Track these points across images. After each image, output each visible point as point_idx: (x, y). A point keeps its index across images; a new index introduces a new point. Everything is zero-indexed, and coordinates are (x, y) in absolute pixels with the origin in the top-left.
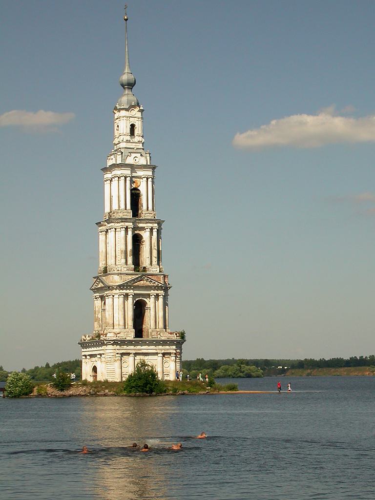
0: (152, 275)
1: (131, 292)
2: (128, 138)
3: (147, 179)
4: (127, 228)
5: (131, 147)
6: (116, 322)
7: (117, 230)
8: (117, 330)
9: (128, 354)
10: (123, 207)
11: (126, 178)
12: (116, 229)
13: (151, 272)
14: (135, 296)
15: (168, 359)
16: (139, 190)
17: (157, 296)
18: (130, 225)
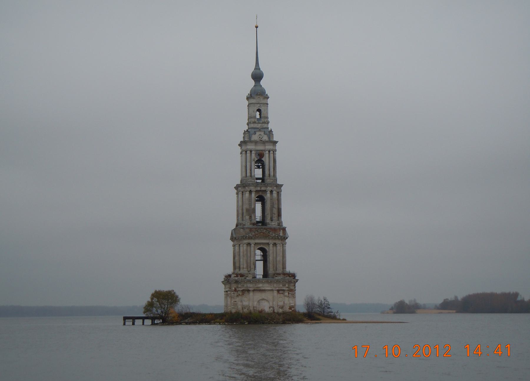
0: (271, 229)
1: (252, 242)
3: (269, 151)
4: (250, 192)
6: (241, 266)
8: (242, 271)
9: (248, 291)
10: (248, 174)
11: (251, 151)
12: (243, 192)
14: (256, 244)
15: (282, 295)
16: (262, 161)
17: (275, 244)
18: (253, 188)
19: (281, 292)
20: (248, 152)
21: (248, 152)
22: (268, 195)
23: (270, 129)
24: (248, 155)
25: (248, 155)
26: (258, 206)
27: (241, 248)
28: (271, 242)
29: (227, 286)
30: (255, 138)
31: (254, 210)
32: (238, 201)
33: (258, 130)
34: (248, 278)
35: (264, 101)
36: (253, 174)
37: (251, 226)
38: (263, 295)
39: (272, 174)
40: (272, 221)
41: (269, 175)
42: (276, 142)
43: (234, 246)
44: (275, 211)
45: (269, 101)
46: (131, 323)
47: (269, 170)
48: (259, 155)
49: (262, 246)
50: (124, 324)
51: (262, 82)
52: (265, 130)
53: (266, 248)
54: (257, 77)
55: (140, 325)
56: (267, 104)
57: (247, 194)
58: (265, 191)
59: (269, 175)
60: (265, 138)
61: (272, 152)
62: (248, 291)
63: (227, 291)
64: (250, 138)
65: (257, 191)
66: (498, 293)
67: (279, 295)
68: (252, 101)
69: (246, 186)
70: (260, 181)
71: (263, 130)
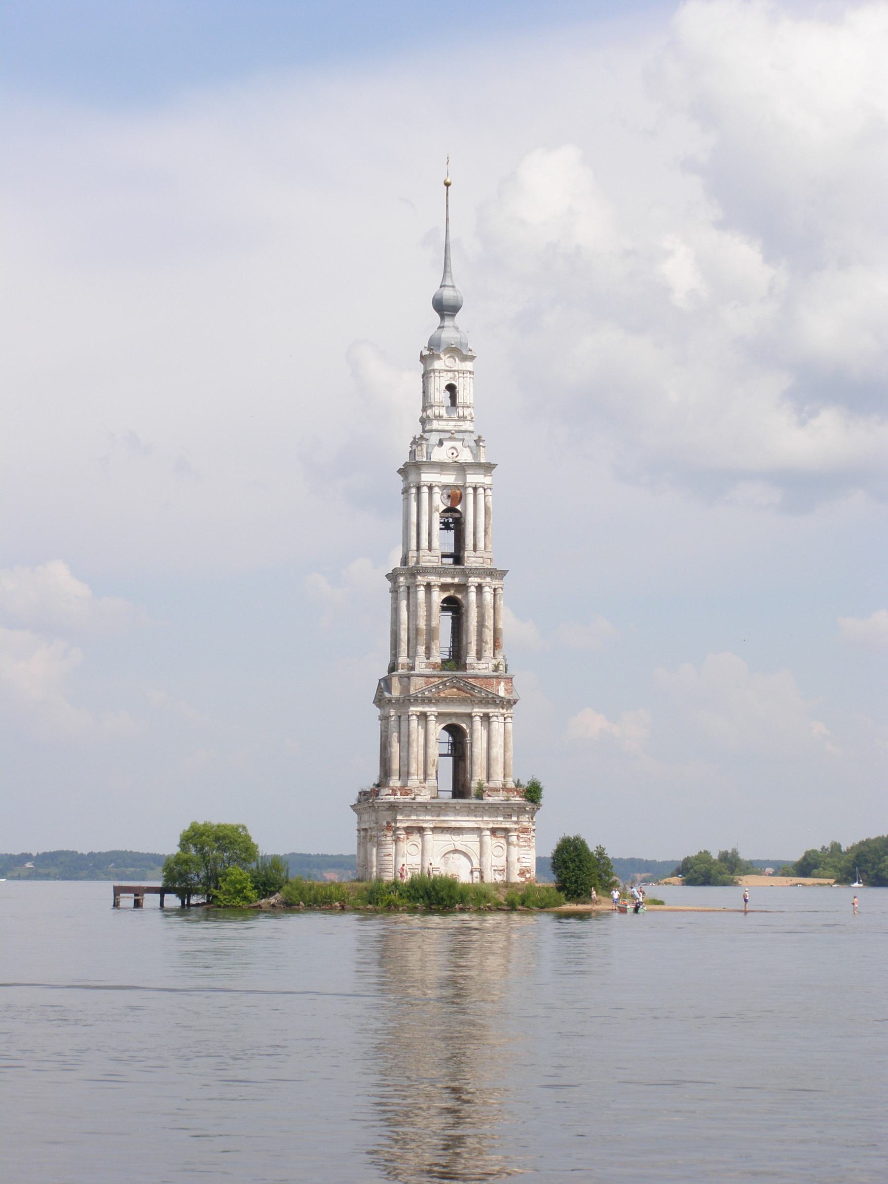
0: (476, 677)
2: (443, 412)
4: (428, 587)
5: (447, 428)
7: (411, 590)
11: (431, 488)
13: (476, 672)
14: (440, 716)
16: (457, 511)
17: (486, 718)
18: (434, 580)
19: (499, 834)
20: (425, 490)
21: (425, 490)
22: (473, 596)
26: (444, 623)
28: (478, 711)
29: (366, 817)
31: (431, 634)
32: (396, 611)
33: (448, 435)
34: (419, 799)
37: (429, 671)
38: (458, 841)
39: (481, 545)
40: (479, 659)
41: (475, 546)
43: (385, 719)
44: (489, 635)
46: (131, 903)
47: (475, 534)
48: (449, 496)
49: (454, 721)
50: (116, 905)
53: (464, 726)
55: (155, 909)
57: (421, 593)
58: (463, 588)
59: (475, 546)
60: (466, 456)
61: (481, 491)
62: (421, 830)
63: (365, 830)
65: (444, 587)
67: (495, 840)
69: (419, 573)
70: (451, 561)
71: (460, 436)
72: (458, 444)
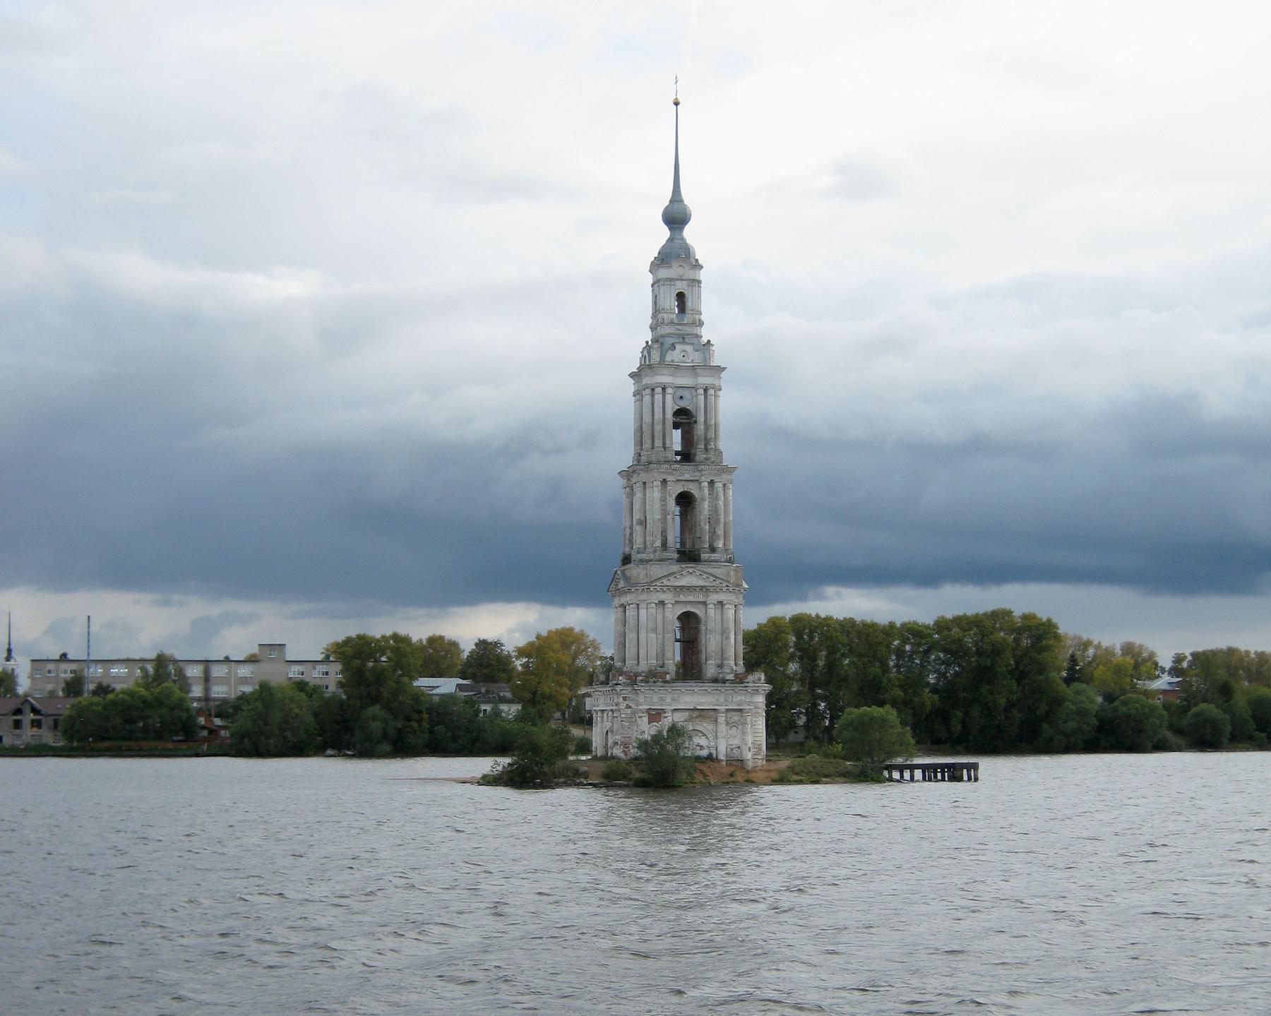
11: (664, 389)
20: (659, 390)
23: (704, 340)
24: (658, 397)
25: (658, 397)
27: (643, 613)
30: (674, 356)
35: (691, 274)
36: (668, 442)
42: (720, 369)
45: (702, 275)
51: (689, 233)
52: (694, 341)
54: (676, 218)
56: (699, 282)
64: (662, 357)
66: (969, 614)
68: (664, 273)
72: (689, 348)
